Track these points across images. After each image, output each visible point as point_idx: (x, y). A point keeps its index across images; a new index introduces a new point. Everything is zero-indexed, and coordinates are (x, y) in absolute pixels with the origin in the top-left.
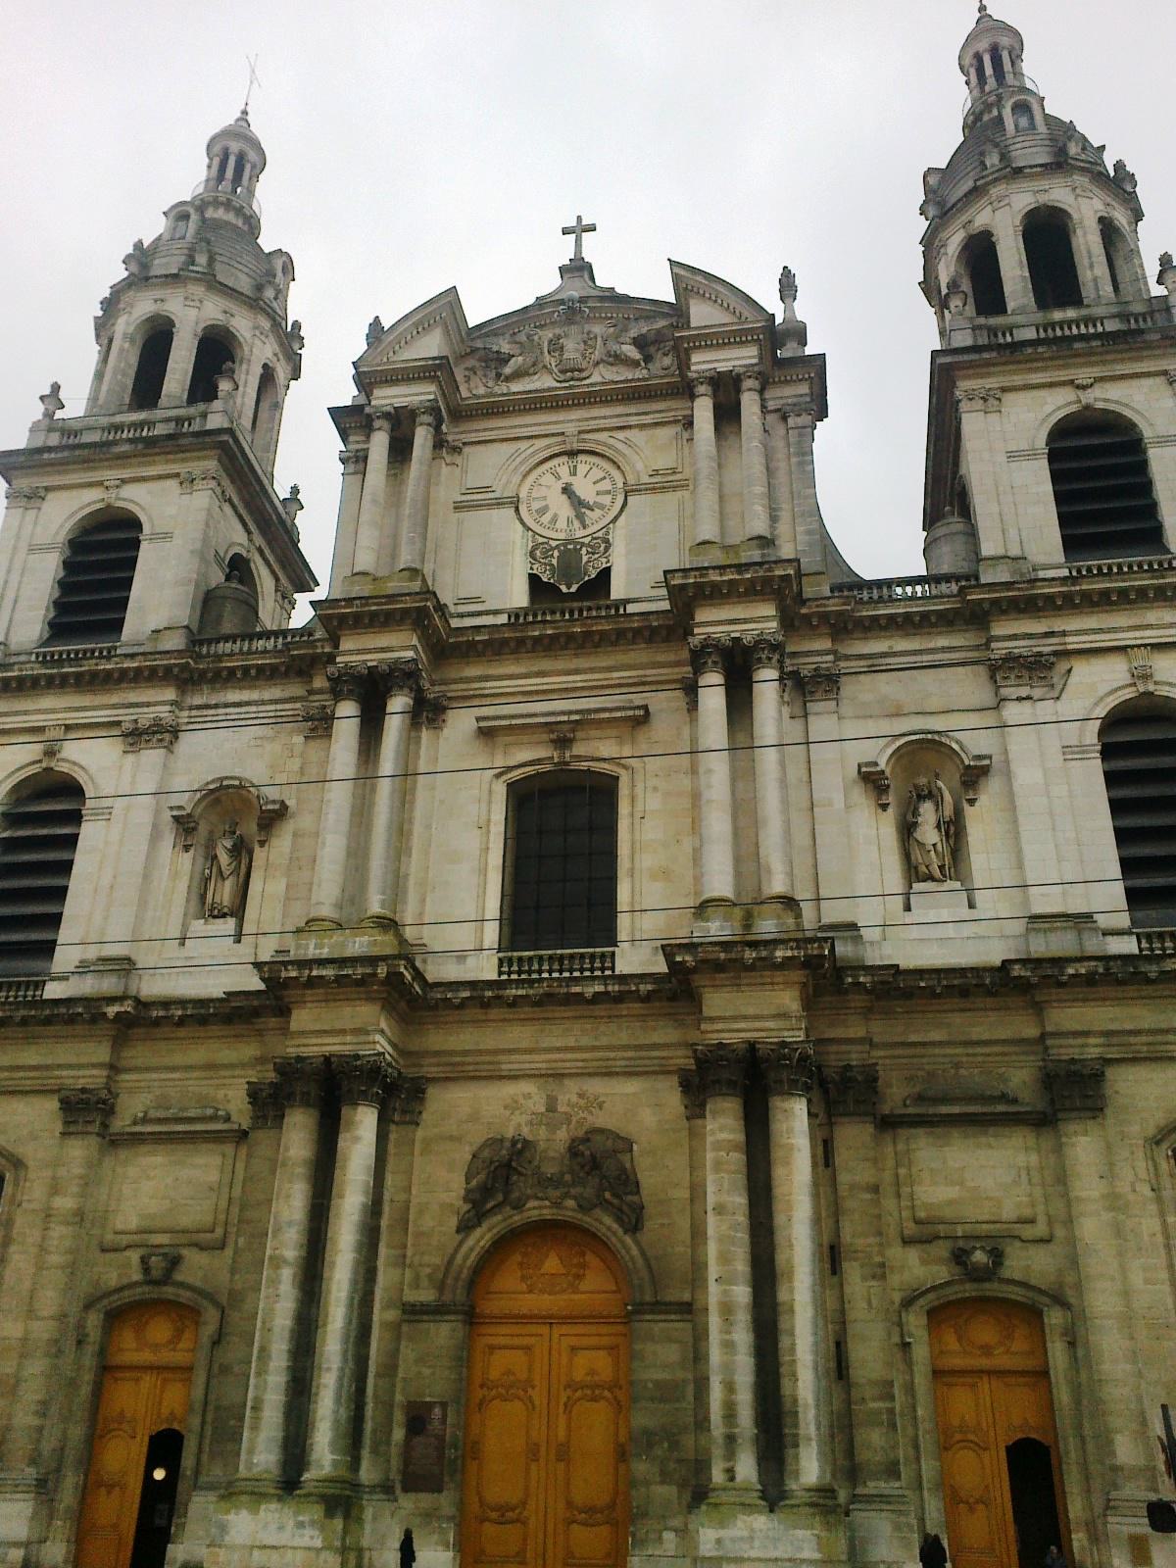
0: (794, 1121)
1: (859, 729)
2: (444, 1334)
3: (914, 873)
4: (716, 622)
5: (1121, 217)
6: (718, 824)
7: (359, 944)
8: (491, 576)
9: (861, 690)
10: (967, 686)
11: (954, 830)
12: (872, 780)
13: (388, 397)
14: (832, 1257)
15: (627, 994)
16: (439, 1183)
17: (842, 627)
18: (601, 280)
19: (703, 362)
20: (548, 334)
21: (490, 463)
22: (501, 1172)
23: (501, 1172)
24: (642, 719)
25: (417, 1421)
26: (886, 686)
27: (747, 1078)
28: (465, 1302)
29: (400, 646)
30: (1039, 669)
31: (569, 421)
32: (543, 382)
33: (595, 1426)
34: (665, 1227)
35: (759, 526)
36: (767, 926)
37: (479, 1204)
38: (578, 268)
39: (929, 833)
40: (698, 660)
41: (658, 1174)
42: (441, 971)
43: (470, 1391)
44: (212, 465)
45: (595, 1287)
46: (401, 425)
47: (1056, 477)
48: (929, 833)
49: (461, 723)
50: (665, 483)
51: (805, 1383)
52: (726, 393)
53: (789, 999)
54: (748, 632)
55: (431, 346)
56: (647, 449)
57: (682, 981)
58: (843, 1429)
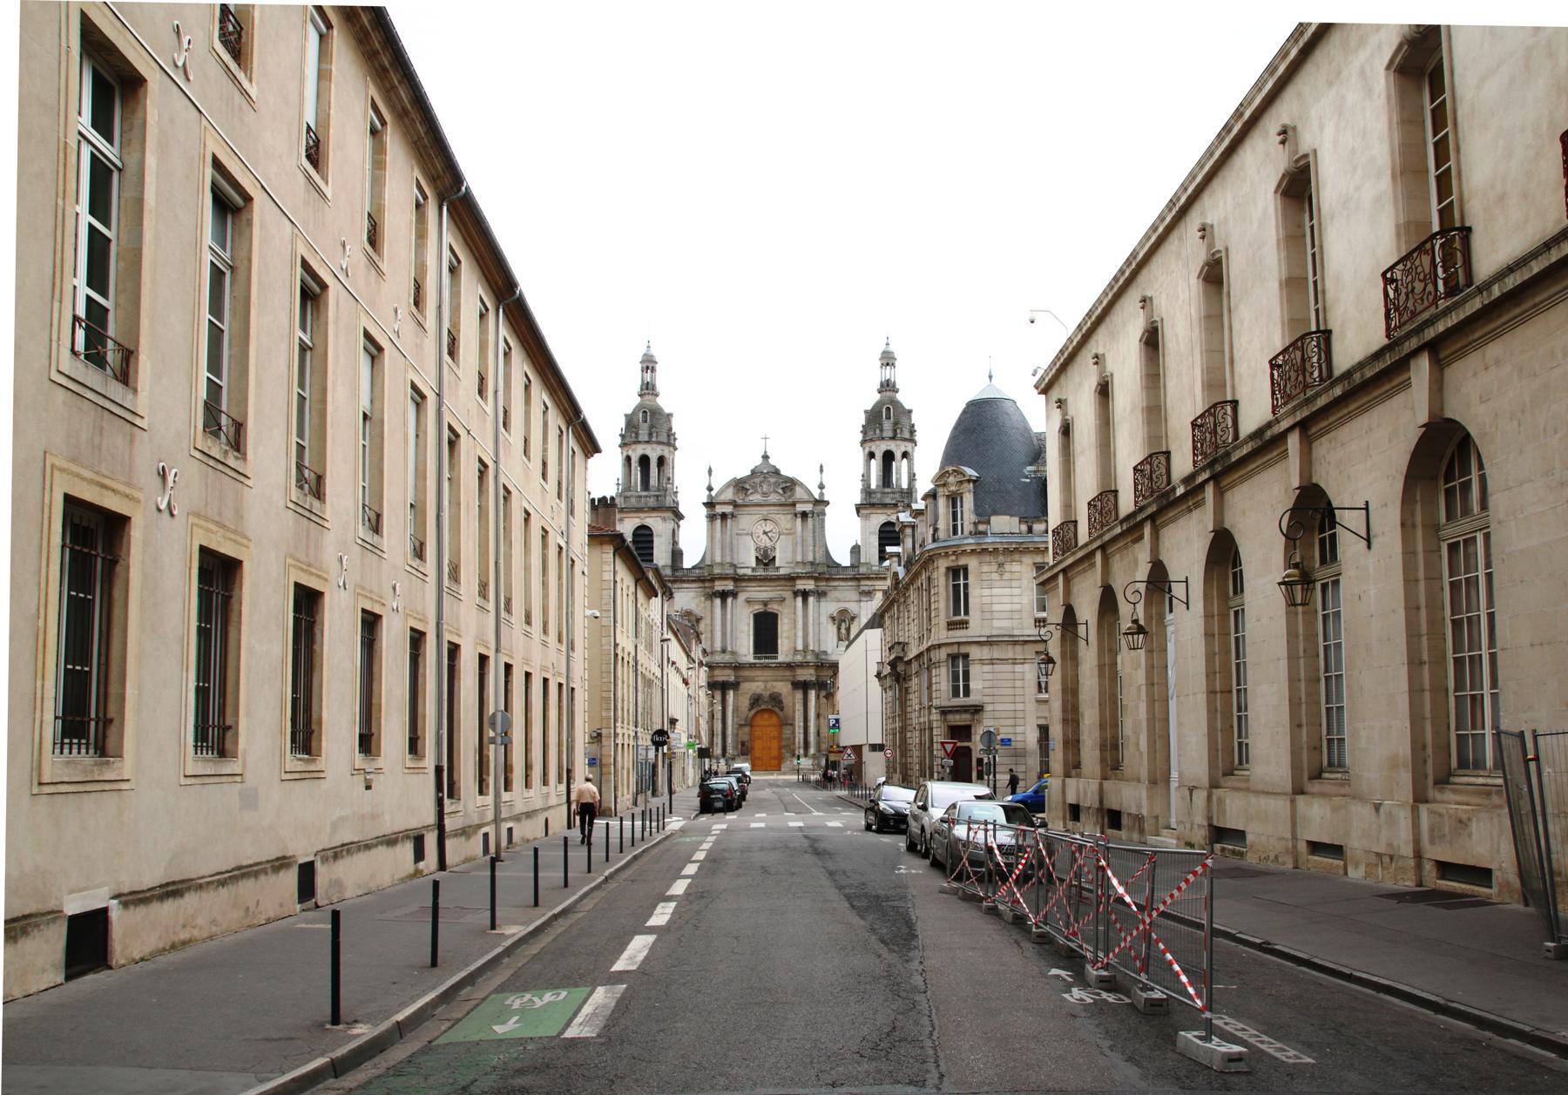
0: (812, 694)
1: (830, 607)
2: (747, 729)
3: (840, 639)
4: (802, 585)
5: (909, 449)
6: (800, 634)
7: (727, 658)
8: (747, 559)
9: (833, 595)
10: (854, 595)
11: (848, 630)
12: (833, 619)
13: (719, 509)
14: (818, 716)
15: (781, 666)
16: (745, 702)
17: (828, 580)
18: (771, 461)
19: (800, 508)
20: (757, 480)
21: (747, 521)
22: (756, 700)
23: (756, 700)
24: (784, 600)
25: (743, 744)
26: (836, 594)
27: (804, 686)
28: (750, 723)
29: (729, 586)
30: (869, 594)
31: (764, 510)
32: (756, 498)
33: (775, 744)
34: (788, 710)
35: (811, 559)
36: (810, 658)
37: (752, 706)
38: (766, 457)
39: (843, 631)
40: (796, 594)
41: (787, 701)
42: (743, 660)
43: (752, 739)
44: (670, 515)
45: (774, 720)
46: (724, 516)
47: (880, 538)
48: (843, 631)
49: (742, 597)
50: (791, 533)
51: (812, 738)
52: (804, 515)
53: (812, 671)
54: (808, 588)
55: (729, 495)
56: (784, 520)
57: (790, 666)
58: (818, 744)
